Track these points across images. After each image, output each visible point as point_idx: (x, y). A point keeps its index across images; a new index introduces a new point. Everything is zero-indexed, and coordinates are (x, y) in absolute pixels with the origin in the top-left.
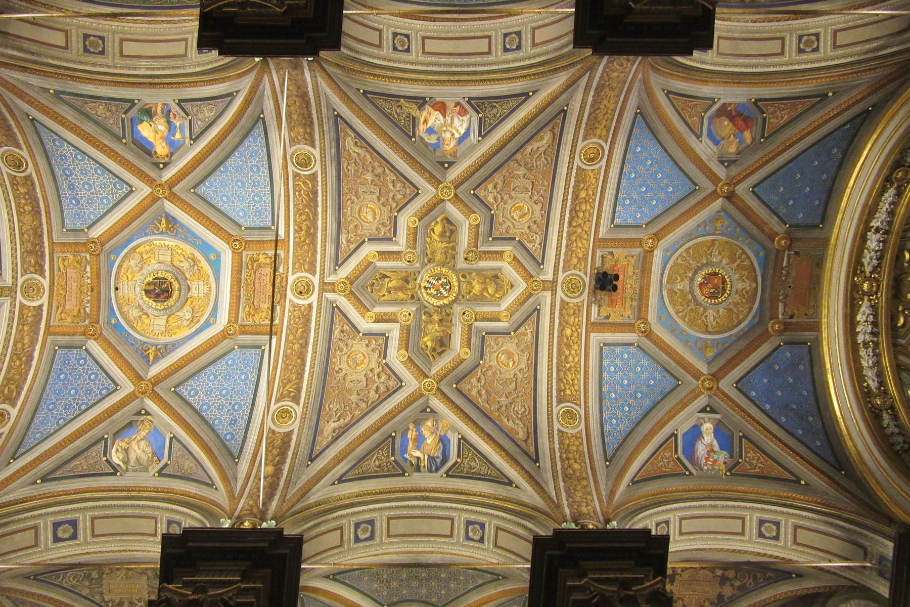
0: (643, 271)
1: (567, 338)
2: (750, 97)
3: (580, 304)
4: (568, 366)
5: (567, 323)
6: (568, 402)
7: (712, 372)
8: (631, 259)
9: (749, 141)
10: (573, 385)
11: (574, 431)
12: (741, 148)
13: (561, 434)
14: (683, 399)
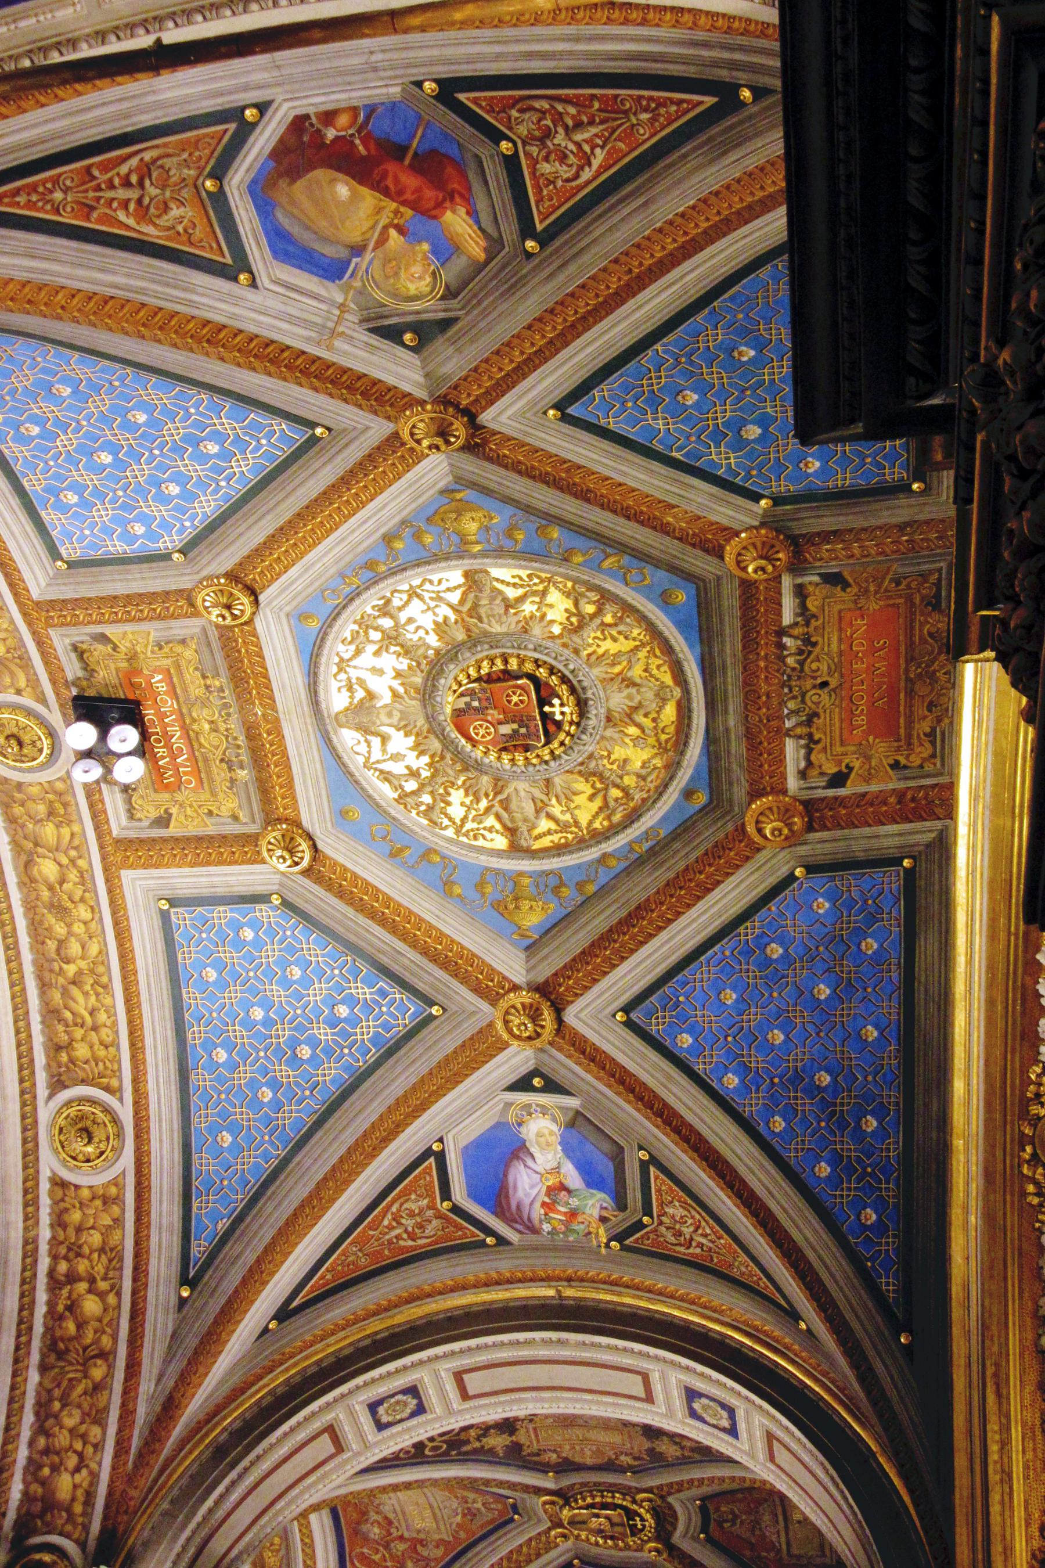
0: (238, 680)
1: (51, 888)
2: (416, 74)
3: (60, 786)
4: (71, 969)
5: (36, 844)
6: (83, 1082)
7: (541, 979)
8: (179, 649)
9: (475, 248)
10: (95, 1028)
11: (99, 1180)
12: (449, 275)
13: (59, 1193)
14: (447, 1060)
